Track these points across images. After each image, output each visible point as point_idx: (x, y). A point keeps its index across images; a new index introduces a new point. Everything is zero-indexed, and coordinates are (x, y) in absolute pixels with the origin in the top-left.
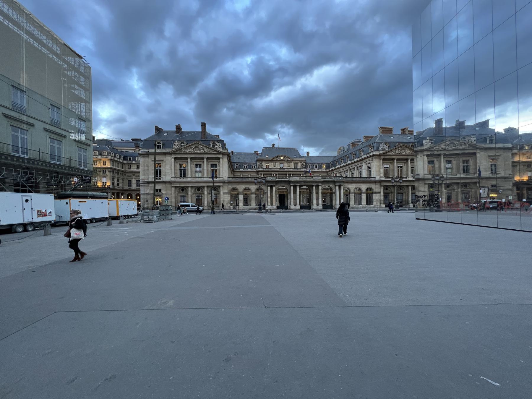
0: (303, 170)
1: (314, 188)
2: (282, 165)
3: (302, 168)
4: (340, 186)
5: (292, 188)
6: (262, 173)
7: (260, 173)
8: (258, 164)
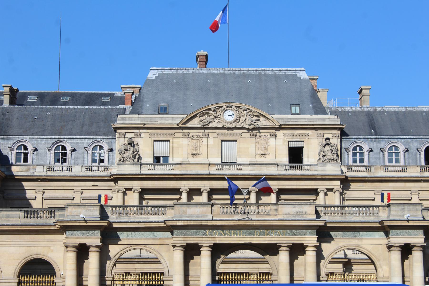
0: (332, 169)
6: (137, 185)
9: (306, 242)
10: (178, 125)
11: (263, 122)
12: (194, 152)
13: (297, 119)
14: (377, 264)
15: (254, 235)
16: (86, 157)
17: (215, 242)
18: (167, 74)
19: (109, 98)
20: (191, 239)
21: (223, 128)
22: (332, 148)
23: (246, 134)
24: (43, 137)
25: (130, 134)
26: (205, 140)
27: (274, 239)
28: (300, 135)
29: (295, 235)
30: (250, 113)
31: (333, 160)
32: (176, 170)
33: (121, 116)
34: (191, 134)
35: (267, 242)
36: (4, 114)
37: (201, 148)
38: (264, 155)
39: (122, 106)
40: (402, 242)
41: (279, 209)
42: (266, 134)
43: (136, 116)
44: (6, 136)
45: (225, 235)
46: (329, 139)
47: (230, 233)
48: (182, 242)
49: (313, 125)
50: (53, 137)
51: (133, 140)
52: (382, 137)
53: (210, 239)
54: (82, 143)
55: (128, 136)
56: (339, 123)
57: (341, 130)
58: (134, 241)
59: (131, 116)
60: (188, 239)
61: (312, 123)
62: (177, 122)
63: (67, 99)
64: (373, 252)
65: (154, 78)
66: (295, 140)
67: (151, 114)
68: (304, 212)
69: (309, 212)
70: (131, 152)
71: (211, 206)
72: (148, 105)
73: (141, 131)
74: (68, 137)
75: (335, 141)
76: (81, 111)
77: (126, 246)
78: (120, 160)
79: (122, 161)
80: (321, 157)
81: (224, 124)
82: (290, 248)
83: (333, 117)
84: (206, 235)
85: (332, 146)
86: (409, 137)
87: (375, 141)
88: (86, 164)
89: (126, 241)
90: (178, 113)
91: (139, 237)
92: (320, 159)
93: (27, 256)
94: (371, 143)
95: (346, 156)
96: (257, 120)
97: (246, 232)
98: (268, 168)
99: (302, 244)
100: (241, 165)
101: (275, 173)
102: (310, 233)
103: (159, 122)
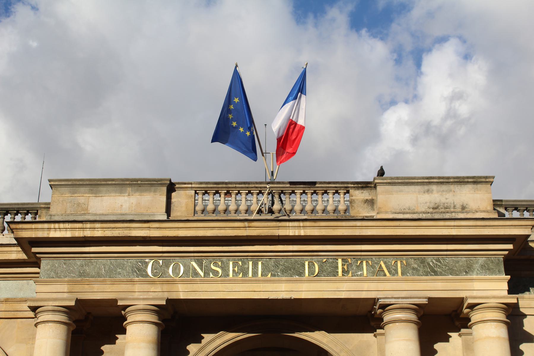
9: (475, 294)
17: (174, 296)
20: (96, 287)
27: (366, 286)
29: (436, 273)
45: (206, 274)
47: (222, 268)
48: (65, 295)
53: (158, 288)
68: (458, 206)
69: (473, 205)
71: (165, 189)
84: (147, 275)
97: (276, 266)
102: (482, 267)
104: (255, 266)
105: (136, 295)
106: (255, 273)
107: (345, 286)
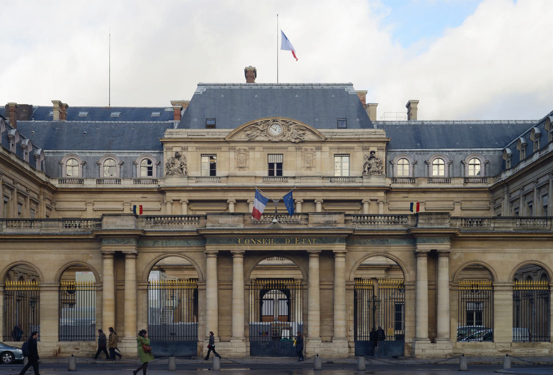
1: (314, 263)
2: (275, 160)
3: (368, 171)
4: (433, 256)
5: (212, 262)
7: (170, 196)
8: (168, 156)
9: (336, 249)
10: (224, 139)
11: (309, 136)
12: (241, 166)
13: (343, 133)
14: (405, 269)
15: (285, 243)
16: (134, 170)
18: (215, 89)
19: (158, 113)
20: (224, 247)
21: (270, 141)
22: (377, 161)
23: (291, 148)
24: (92, 151)
25: (177, 149)
26: (251, 154)
27: (304, 246)
28: (347, 148)
29: (325, 243)
30: (297, 128)
31: (379, 172)
32: (223, 183)
33: (168, 130)
34: (237, 148)
35: (297, 249)
36: (53, 129)
37: (247, 161)
38: (309, 168)
39: (170, 121)
40: (428, 249)
41: (310, 218)
42: (312, 148)
43: (184, 130)
44: (55, 151)
45: (256, 243)
46: (374, 152)
49: (359, 138)
50: (102, 151)
51: (180, 153)
52: (427, 150)
54: (131, 157)
55: (175, 149)
56: (385, 136)
57: (388, 143)
58: (168, 248)
59: (178, 130)
60: (221, 247)
61: (358, 137)
62: (224, 137)
63: (117, 114)
64: (400, 258)
65: (201, 93)
66: (341, 153)
67: (198, 128)
70: (179, 165)
72: (195, 120)
73: (188, 145)
74: (116, 151)
75: (381, 155)
76: (129, 126)
77: (161, 253)
78: (167, 174)
79: (170, 174)
80: (366, 169)
81: (271, 138)
82: (320, 255)
83: (379, 130)
85: (377, 159)
86: (454, 149)
87: (420, 154)
88: (134, 177)
89: (161, 249)
90: (225, 128)
91: (173, 245)
92: (365, 171)
93: (67, 262)
94: (417, 156)
95: (391, 169)
96: (303, 134)
98: (313, 181)
99: (332, 251)
100: (287, 177)
101: (321, 185)
103: (206, 137)
104: (271, 240)
105: (236, 249)
106: (271, 243)
107: (298, 247)
